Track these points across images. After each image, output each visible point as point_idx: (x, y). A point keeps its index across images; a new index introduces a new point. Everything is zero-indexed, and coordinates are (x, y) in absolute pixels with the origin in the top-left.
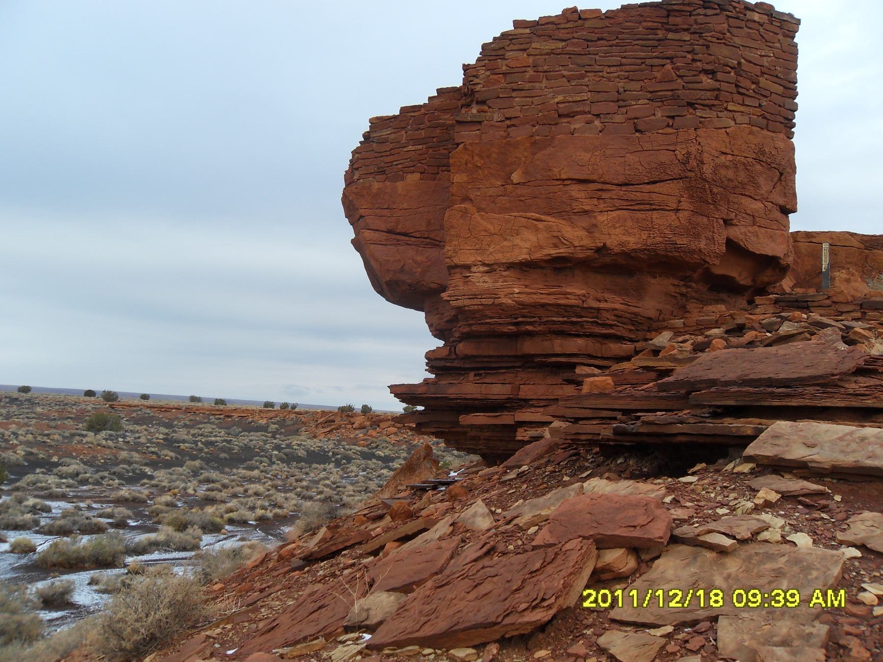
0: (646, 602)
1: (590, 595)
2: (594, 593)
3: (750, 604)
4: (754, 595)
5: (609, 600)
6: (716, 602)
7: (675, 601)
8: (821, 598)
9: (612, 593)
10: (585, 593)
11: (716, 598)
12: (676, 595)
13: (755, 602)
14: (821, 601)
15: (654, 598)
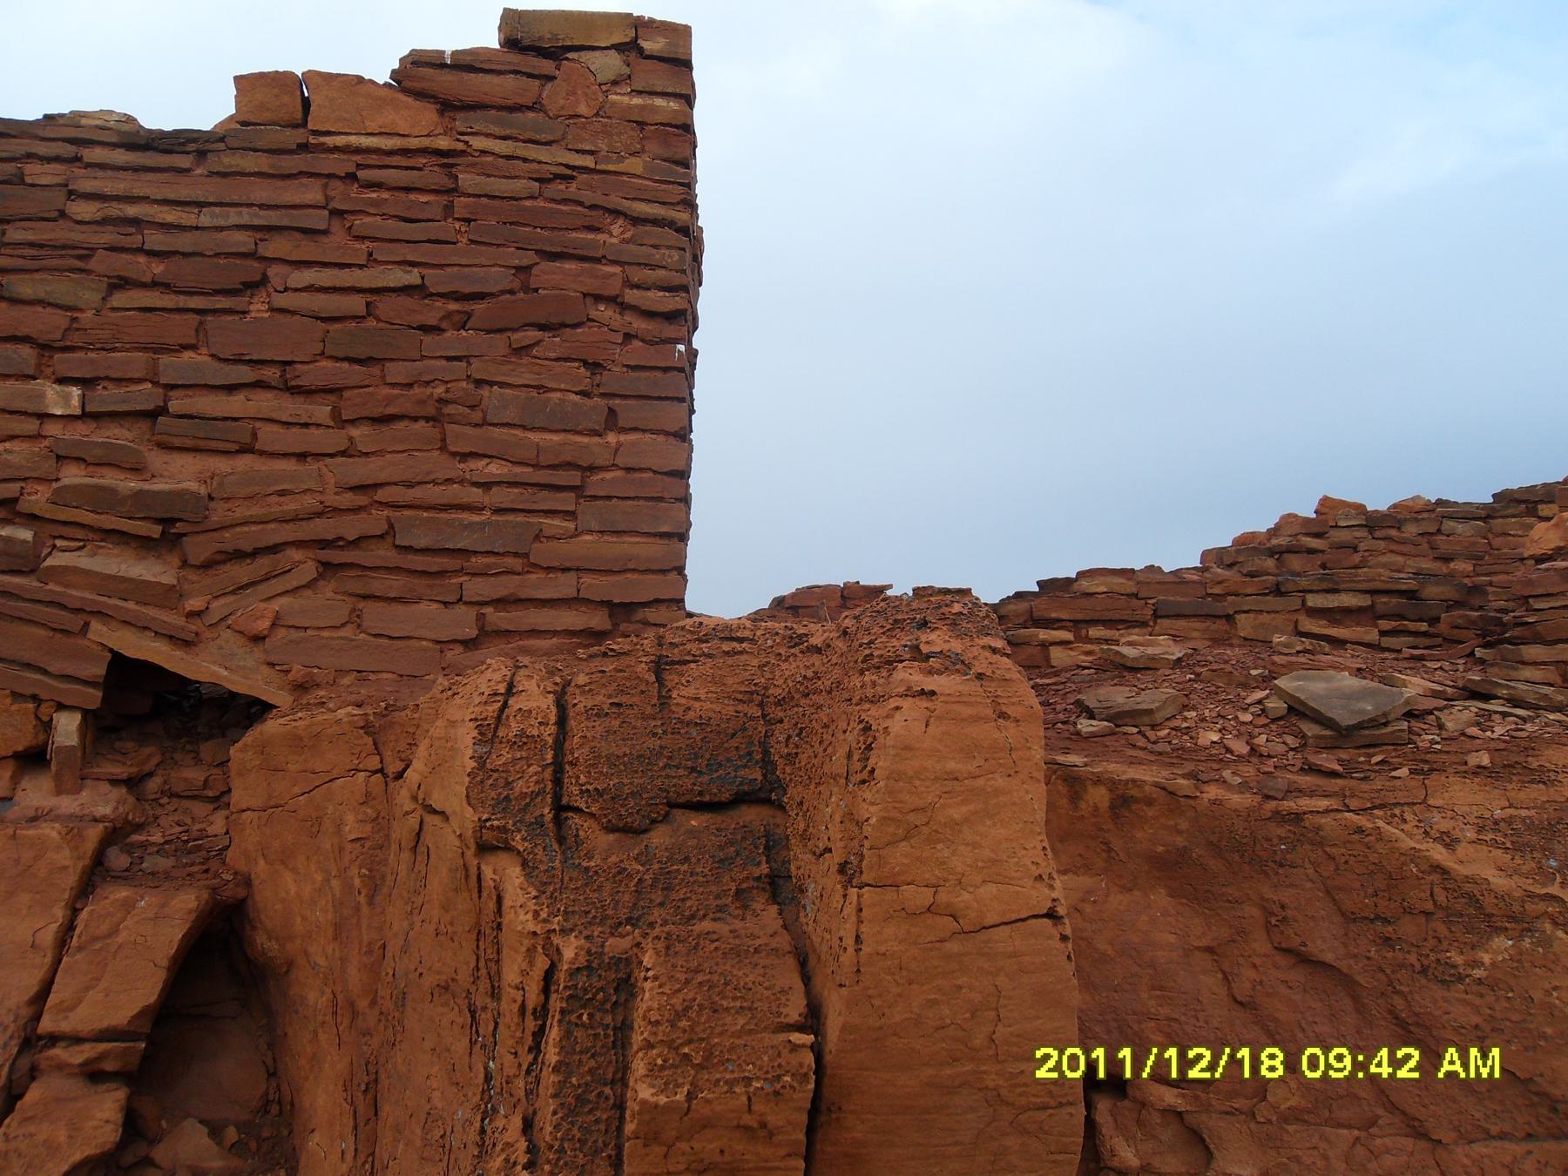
0: (1148, 1070)
1: (1047, 1057)
2: (1055, 1054)
3: (1331, 1073)
4: (1340, 1058)
5: (1082, 1066)
6: (1272, 1069)
7: (1198, 1067)
8: (1458, 1063)
9: (1087, 1052)
10: (1039, 1054)
11: (1272, 1063)
12: (1199, 1057)
13: (1341, 1070)
14: (1457, 1067)
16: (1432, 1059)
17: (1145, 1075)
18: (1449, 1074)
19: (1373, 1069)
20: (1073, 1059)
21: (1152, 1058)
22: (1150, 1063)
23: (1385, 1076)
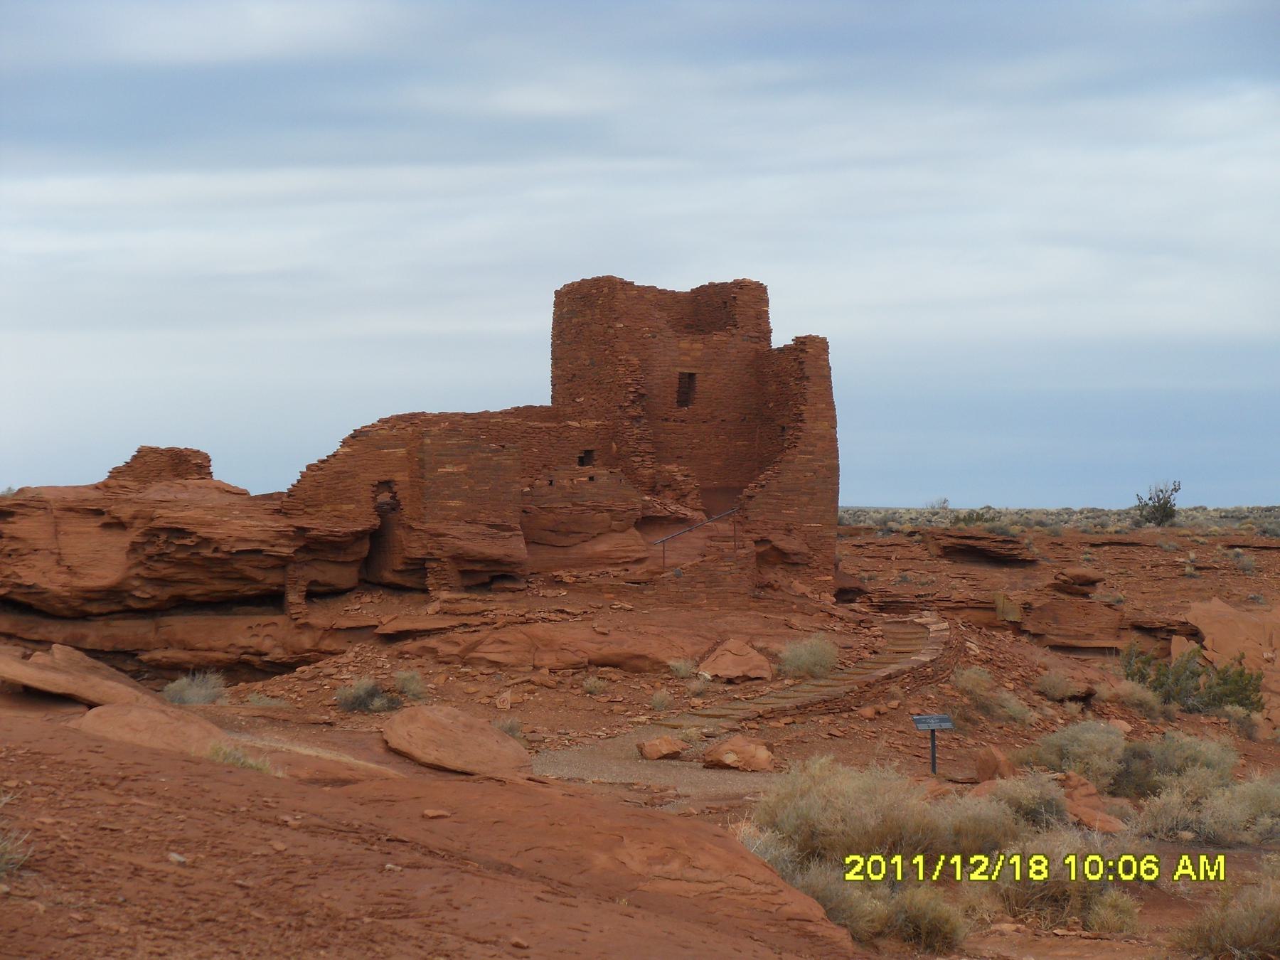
0: (937, 873)
1: (855, 863)
2: (861, 860)
5: (883, 871)
6: (1038, 872)
8: (1190, 868)
9: (888, 857)
10: (848, 860)
11: (1038, 868)
12: (979, 863)
14: (1190, 871)
15: (949, 867)
16: (1168, 866)
17: (935, 878)
20: (876, 866)
21: (941, 863)
22: (938, 868)
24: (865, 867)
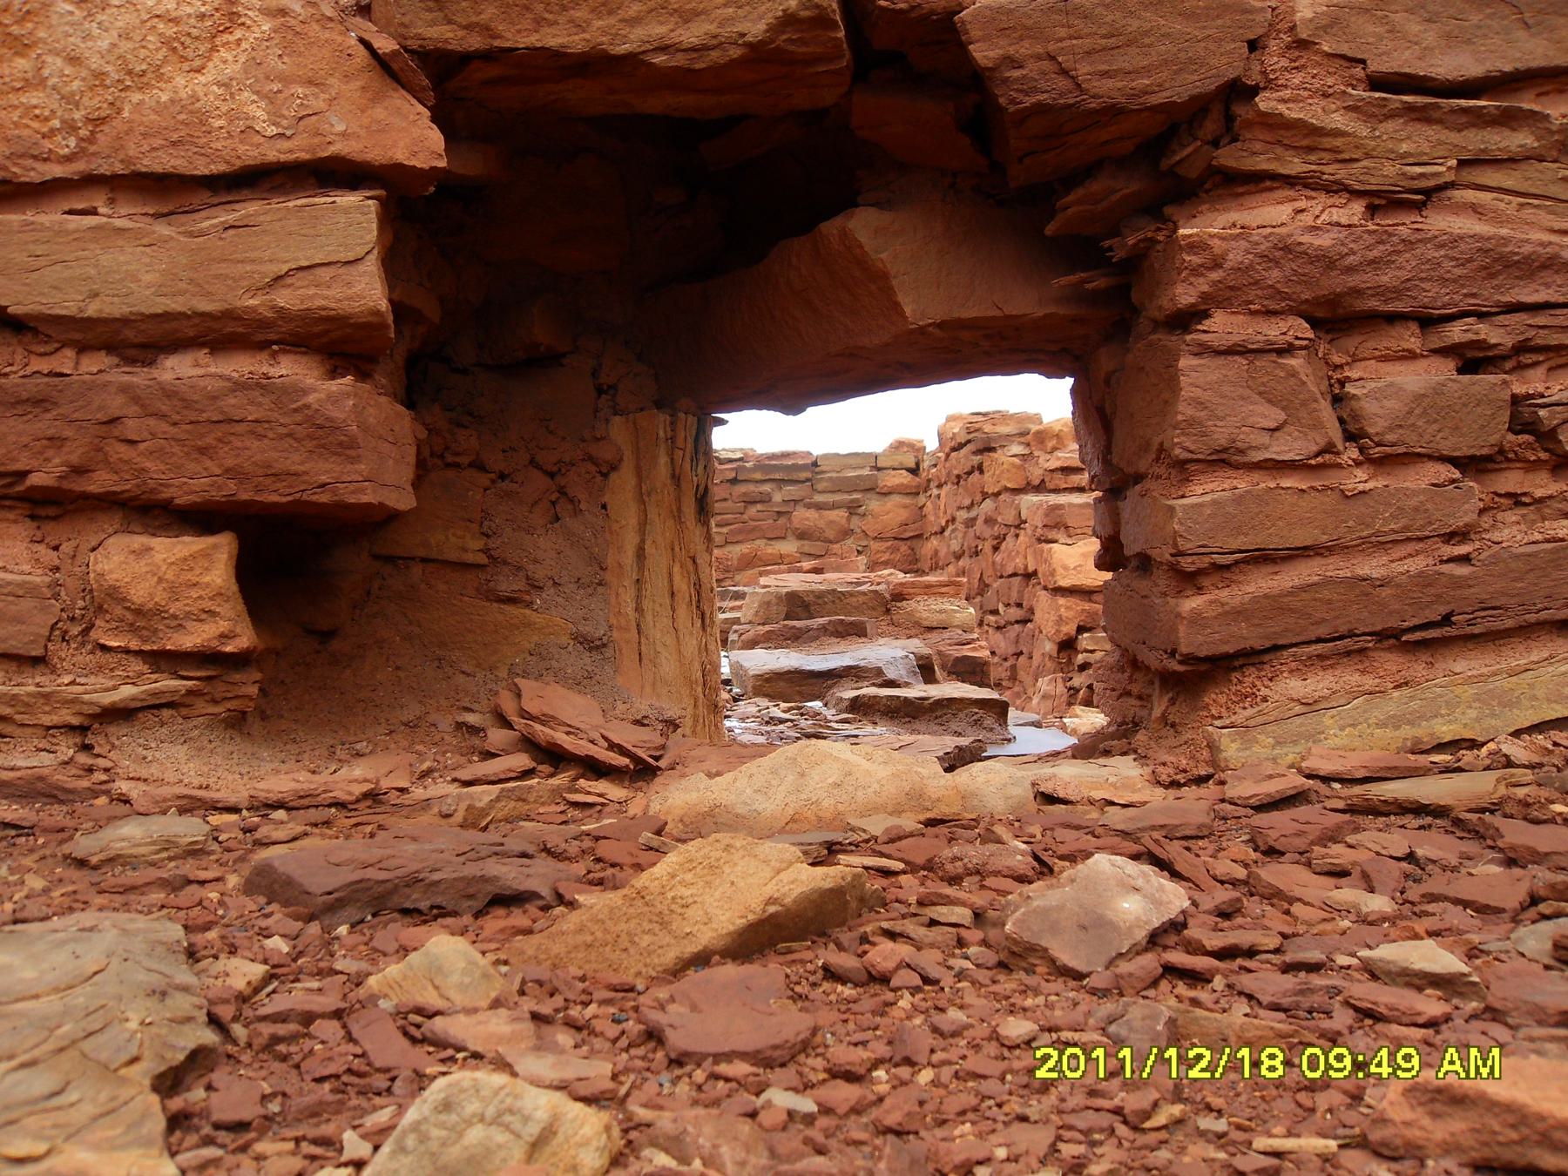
0: (1148, 1070)
2: (1055, 1054)
3: (1331, 1073)
4: (1340, 1058)
6: (1272, 1069)
11: (1272, 1063)
12: (1199, 1057)
13: (1341, 1070)
14: (1457, 1067)
15: (1163, 1061)
17: (1145, 1075)
18: (1447, 1073)
19: (1373, 1069)
23: (1385, 1075)
24: (1060, 1060)
